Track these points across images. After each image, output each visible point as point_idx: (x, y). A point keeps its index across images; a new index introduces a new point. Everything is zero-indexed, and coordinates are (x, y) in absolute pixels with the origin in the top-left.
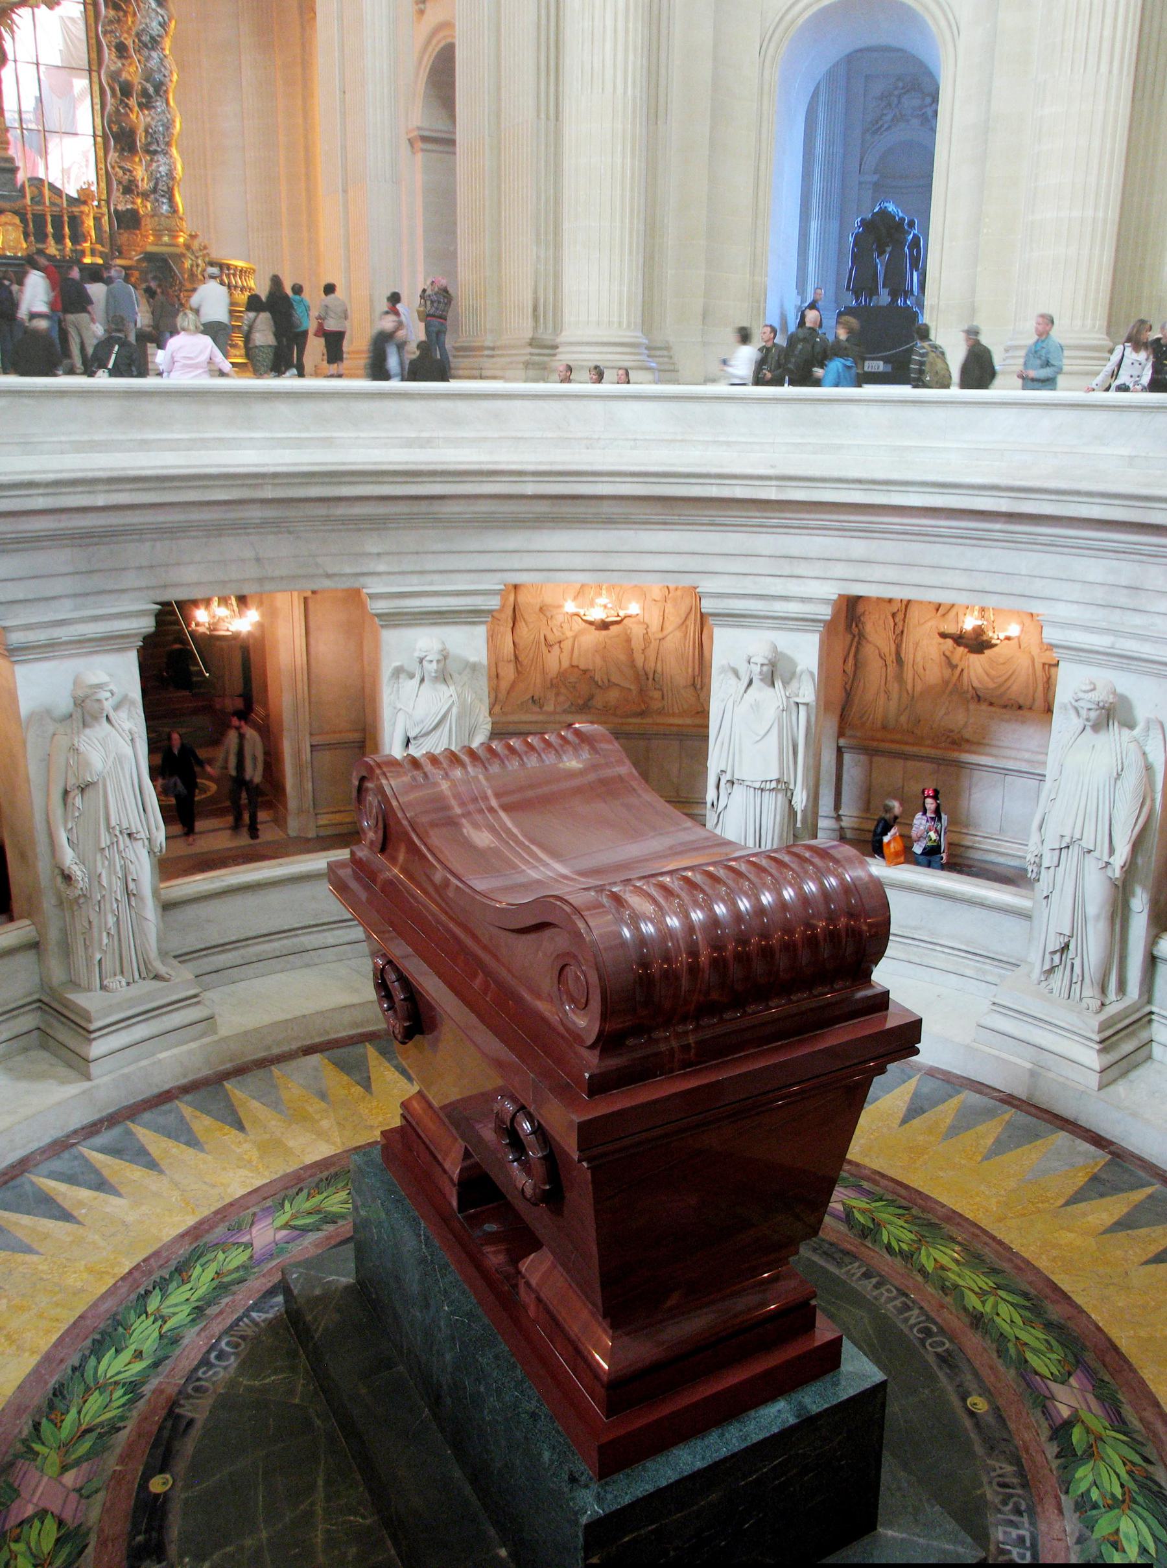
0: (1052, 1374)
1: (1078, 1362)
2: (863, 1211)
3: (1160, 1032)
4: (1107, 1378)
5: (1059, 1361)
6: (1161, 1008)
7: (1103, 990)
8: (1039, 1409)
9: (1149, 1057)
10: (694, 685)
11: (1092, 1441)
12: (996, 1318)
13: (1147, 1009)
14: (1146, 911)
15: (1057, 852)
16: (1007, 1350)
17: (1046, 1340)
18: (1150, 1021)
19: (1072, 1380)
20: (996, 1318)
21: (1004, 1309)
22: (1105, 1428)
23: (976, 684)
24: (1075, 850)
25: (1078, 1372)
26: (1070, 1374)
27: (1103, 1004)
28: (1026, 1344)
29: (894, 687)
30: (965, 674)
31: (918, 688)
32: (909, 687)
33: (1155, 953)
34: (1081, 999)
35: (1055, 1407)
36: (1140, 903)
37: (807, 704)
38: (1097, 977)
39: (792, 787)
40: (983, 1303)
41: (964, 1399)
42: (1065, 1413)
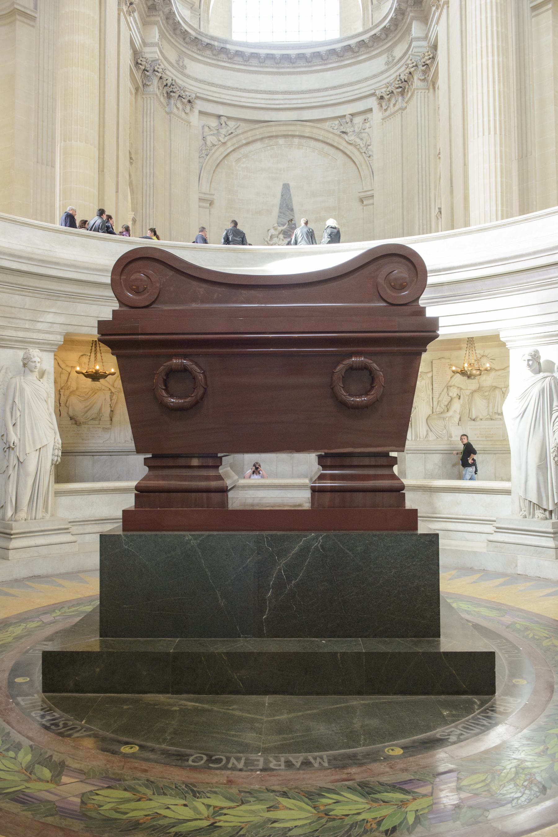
0: (97, 794)
1: (85, 815)
2: (403, 803)
4: (50, 820)
5: (100, 806)
8: (86, 771)
11: (33, 776)
12: (184, 802)
16: (147, 787)
17: (126, 813)
19: (79, 800)
20: (184, 802)
21: (185, 813)
22: (27, 788)
25: (77, 808)
26: (83, 802)
28: (139, 800)
35: (77, 778)
40: (208, 806)
41: (141, 747)
42: (64, 779)
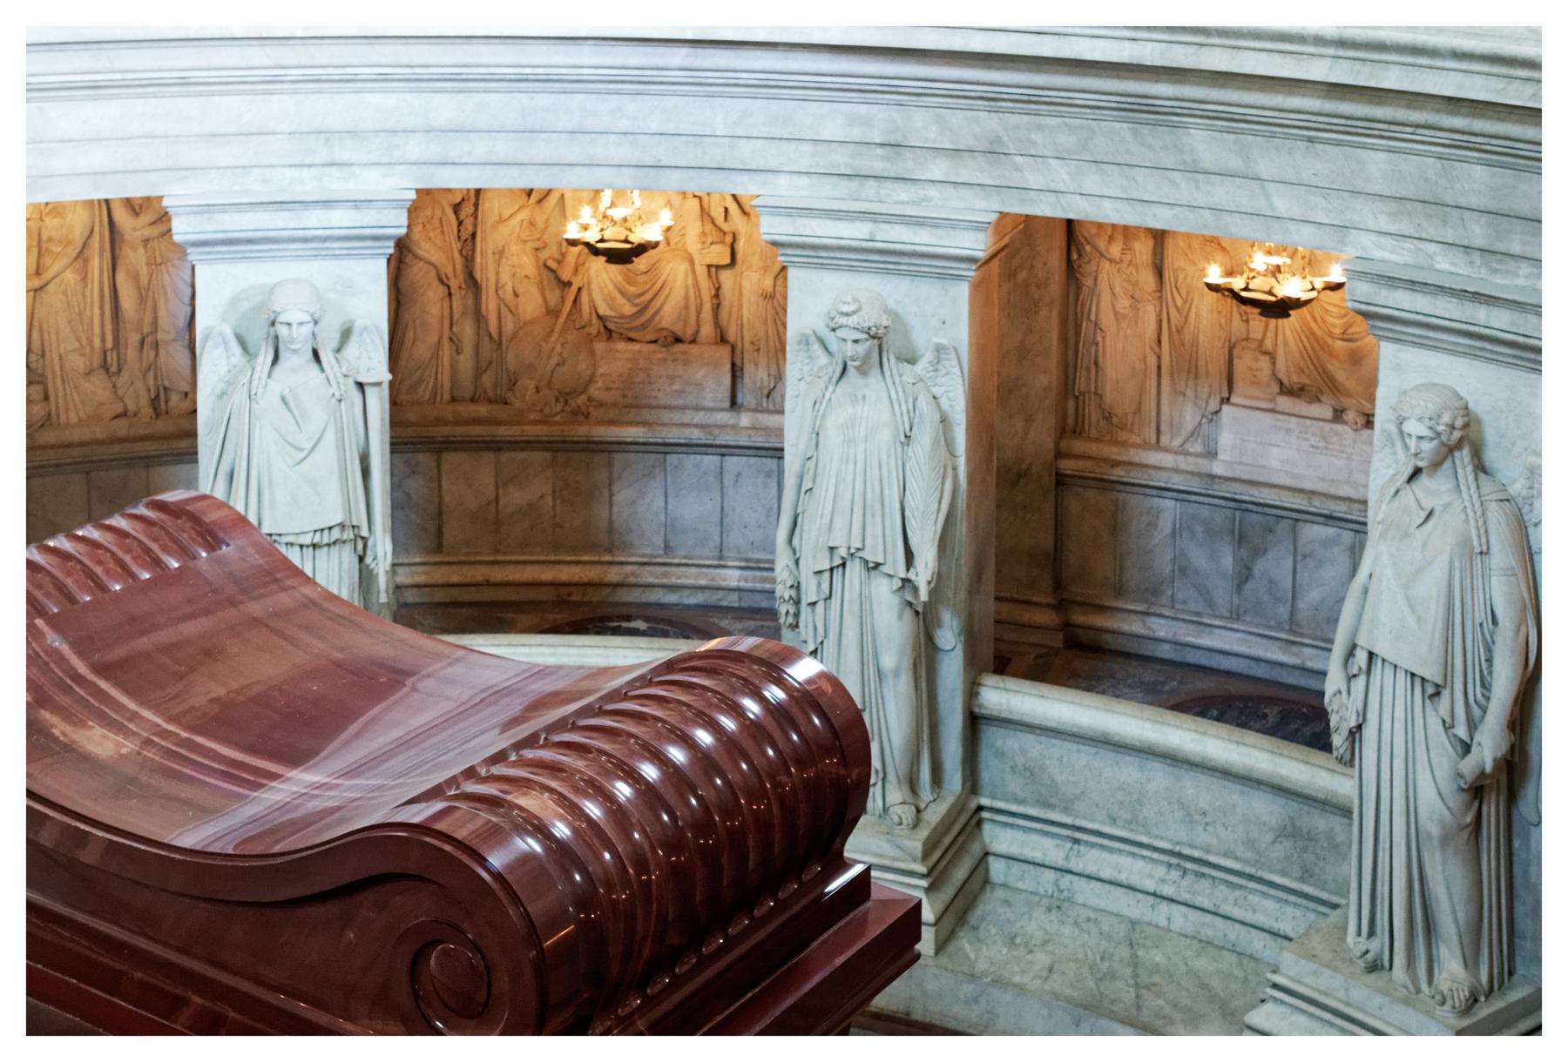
3: (999, 838)
6: (993, 797)
7: (913, 786)
9: (987, 881)
10: (105, 367)
13: (973, 805)
14: (960, 647)
15: (827, 575)
18: (979, 823)
23: (603, 310)
24: (854, 569)
27: (918, 811)
29: (467, 331)
30: (584, 298)
31: (509, 326)
32: (493, 329)
33: (977, 710)
34: (885, 809)
36: (949, 637)
37: (379, 384)
38: (903, 769)
39: (365, 533)
